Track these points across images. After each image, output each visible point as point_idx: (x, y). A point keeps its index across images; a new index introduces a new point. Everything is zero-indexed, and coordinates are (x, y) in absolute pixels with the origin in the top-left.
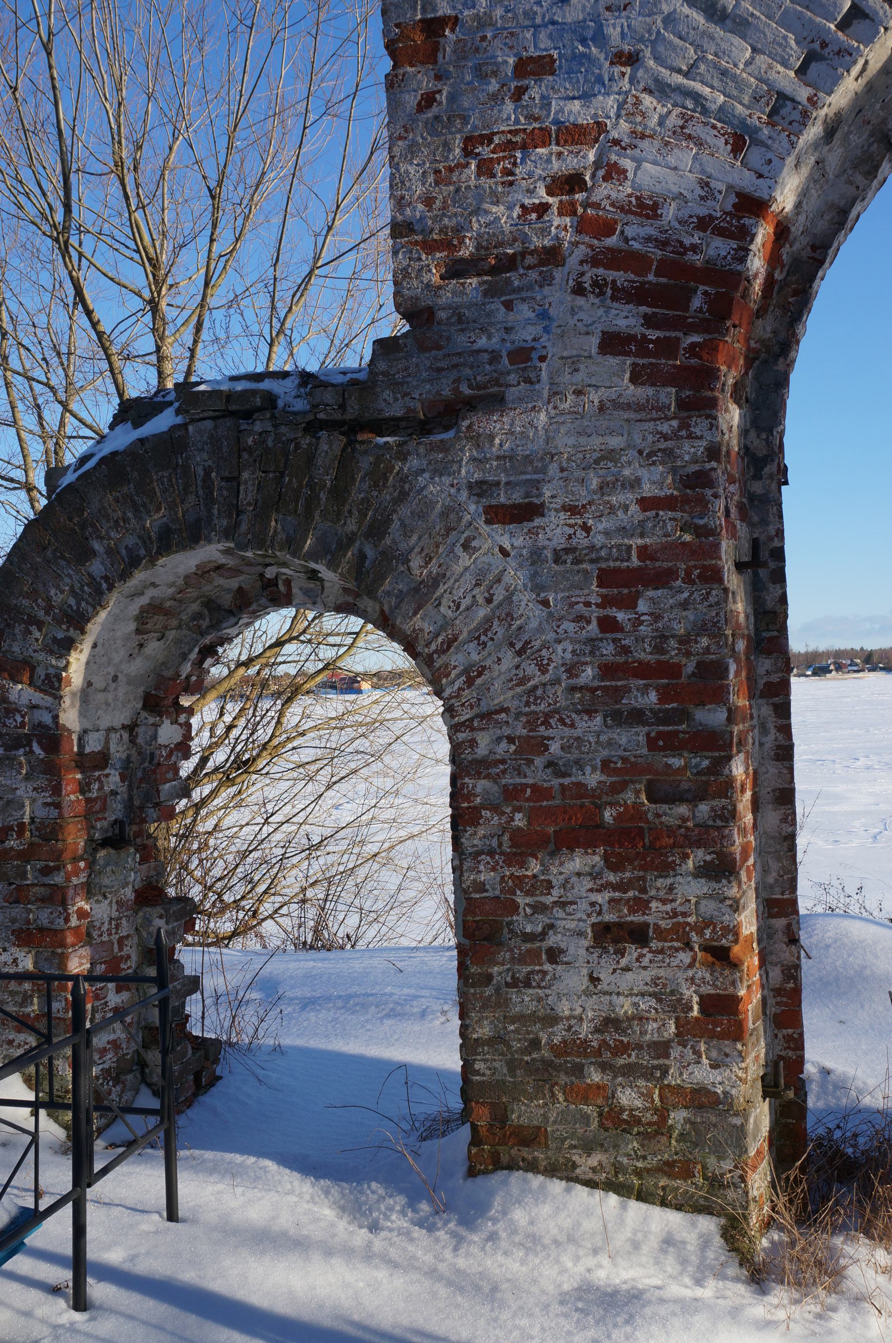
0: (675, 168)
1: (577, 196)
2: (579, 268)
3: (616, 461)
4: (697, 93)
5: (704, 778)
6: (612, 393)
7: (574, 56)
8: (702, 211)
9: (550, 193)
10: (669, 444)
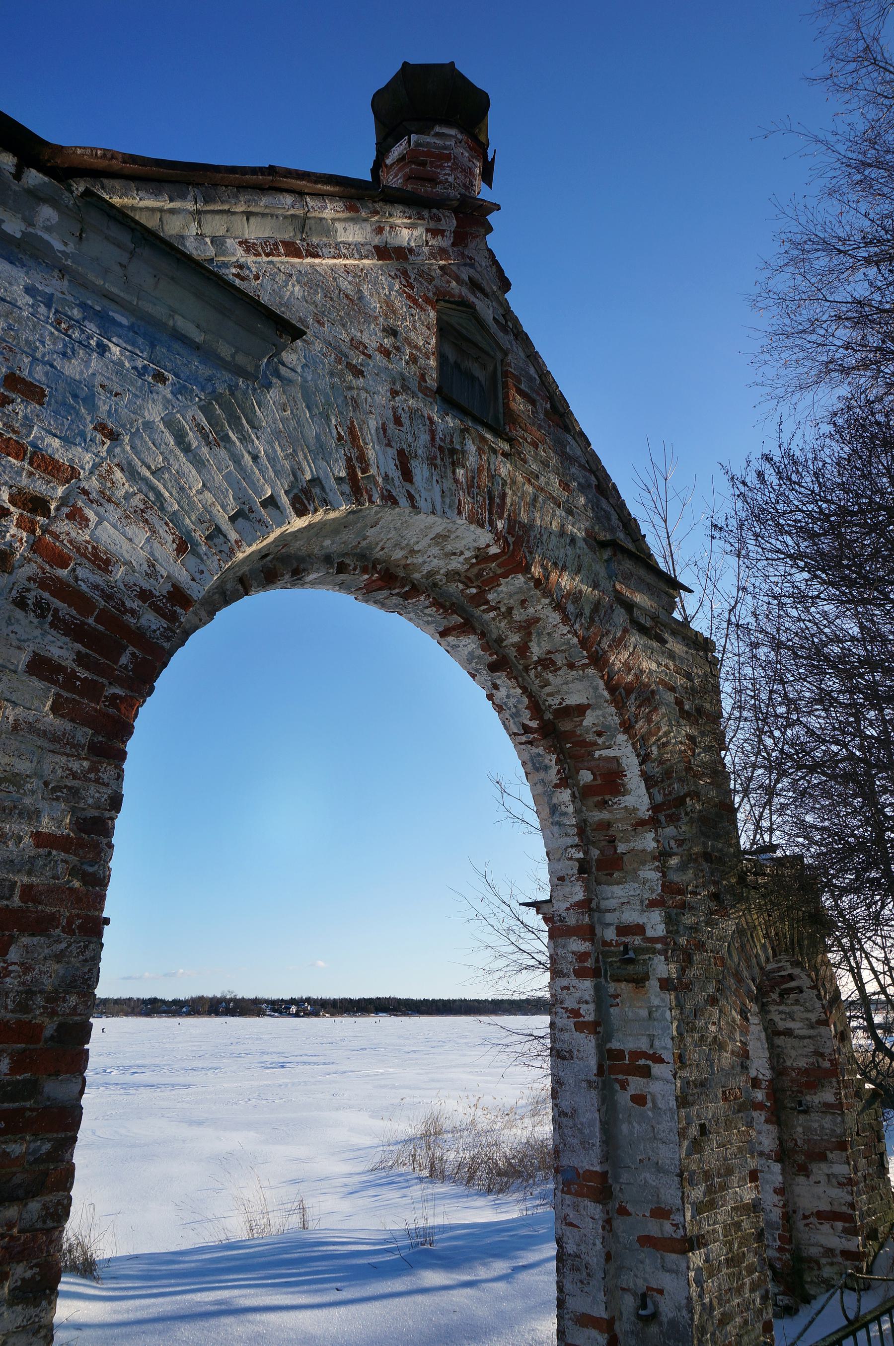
0: (130, 540)
1: (38, 518)
2: (26, 583)
3: (19, 786)
4: (160, 492)
5: (42, 1167)
6: (31, 716)
7: (64, 404)
8: (146, 586)
9: (12, 501)
10: (76, 783)
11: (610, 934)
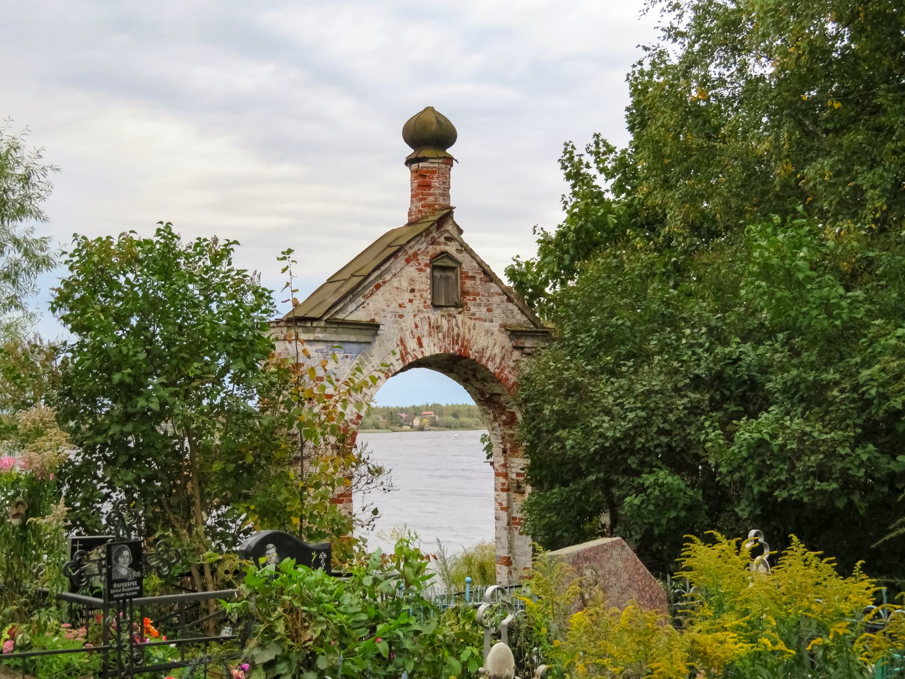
11: (514, 476)
